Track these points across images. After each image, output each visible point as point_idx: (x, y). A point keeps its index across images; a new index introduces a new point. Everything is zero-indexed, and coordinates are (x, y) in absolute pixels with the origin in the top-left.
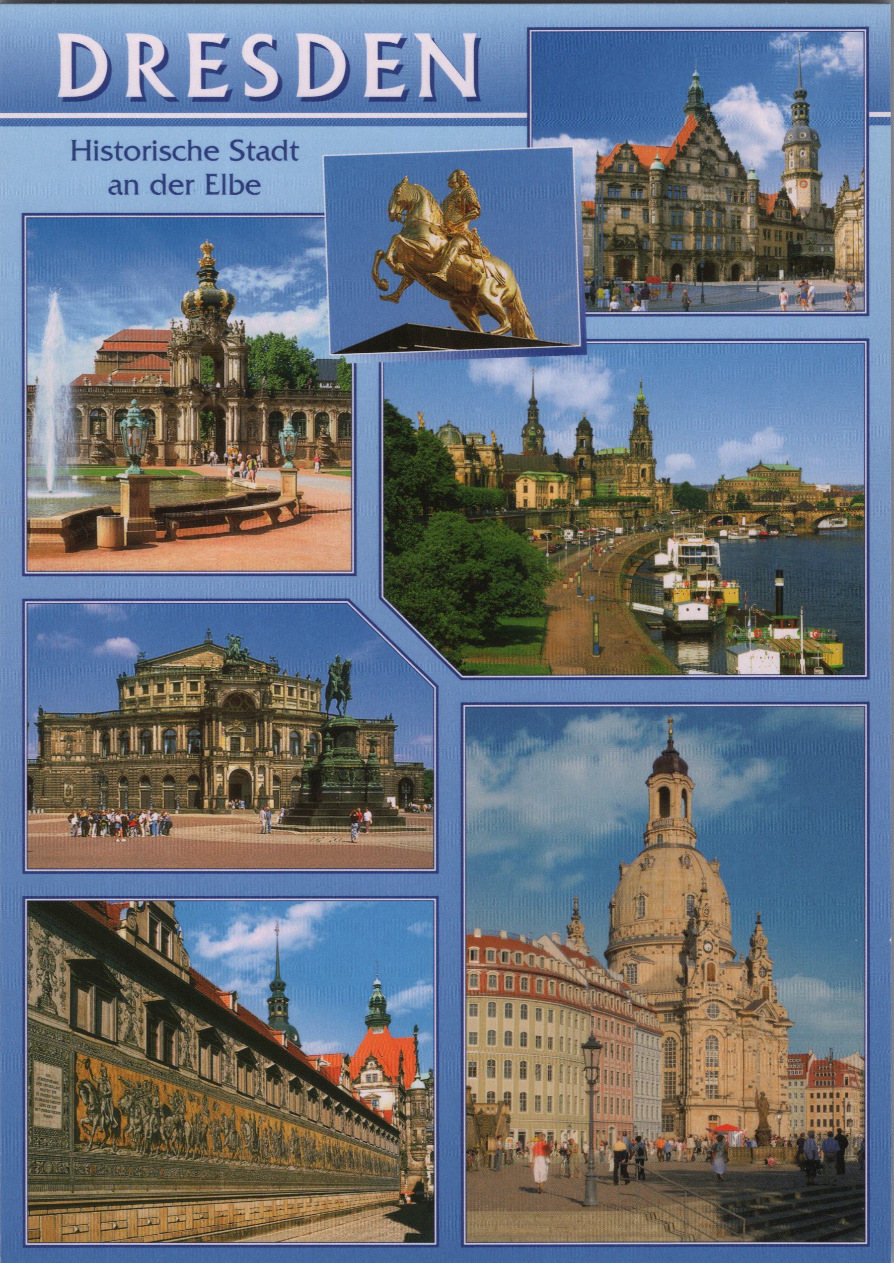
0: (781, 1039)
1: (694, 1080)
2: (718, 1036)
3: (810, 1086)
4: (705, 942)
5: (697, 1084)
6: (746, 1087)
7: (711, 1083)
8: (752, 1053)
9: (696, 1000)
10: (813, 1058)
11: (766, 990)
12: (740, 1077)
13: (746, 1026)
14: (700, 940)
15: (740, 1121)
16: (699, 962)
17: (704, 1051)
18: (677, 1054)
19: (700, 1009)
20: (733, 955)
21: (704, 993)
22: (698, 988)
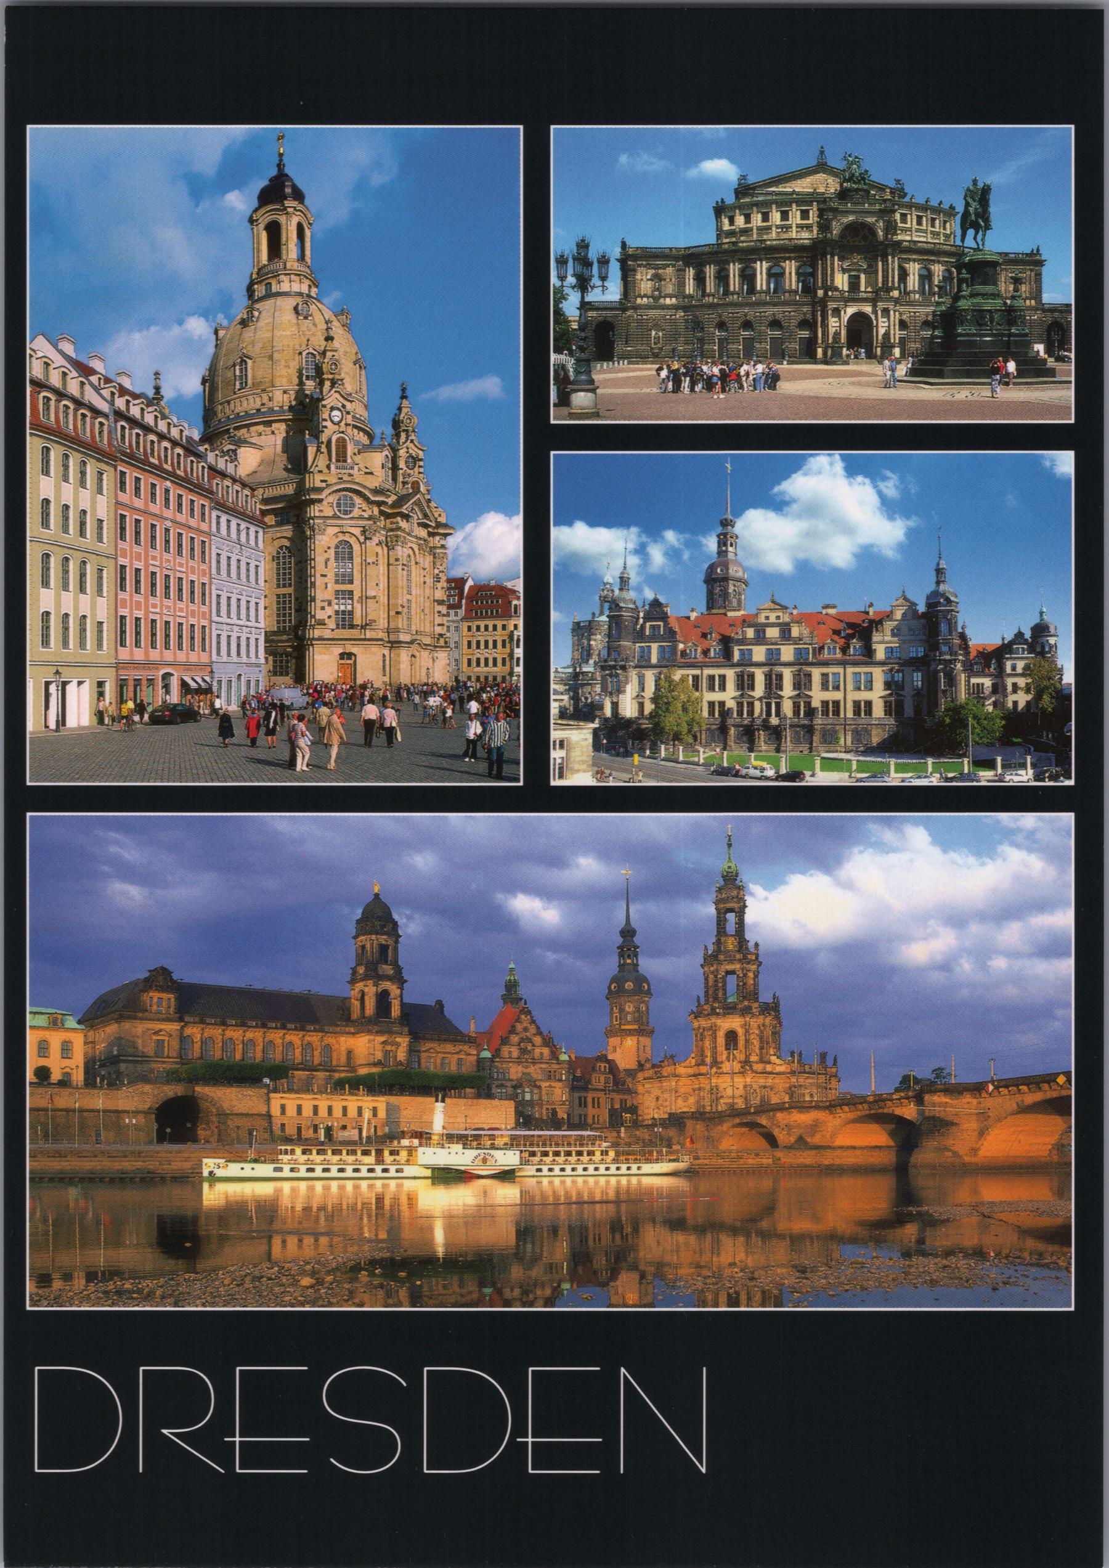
0: (438, 551)
1: (319, 604)
2: (353, 540)
3: (467, 618)
4: (332, 409)
5: (323, 608)
6: (392, 613)
7: (342, 608)
8: (400, 567)
9: (320, 490)
10: (470, 583)
11: (416, 486)
12: (383, 599)
13: (392, 530)
14: (324, 406)
15: (384, 661)
16: (324, 438)
17: (332, 563)
18: (295, 566)
19: (325, 503)
20: (371, 437)
21: (332, 479)
22: (322, 472)
